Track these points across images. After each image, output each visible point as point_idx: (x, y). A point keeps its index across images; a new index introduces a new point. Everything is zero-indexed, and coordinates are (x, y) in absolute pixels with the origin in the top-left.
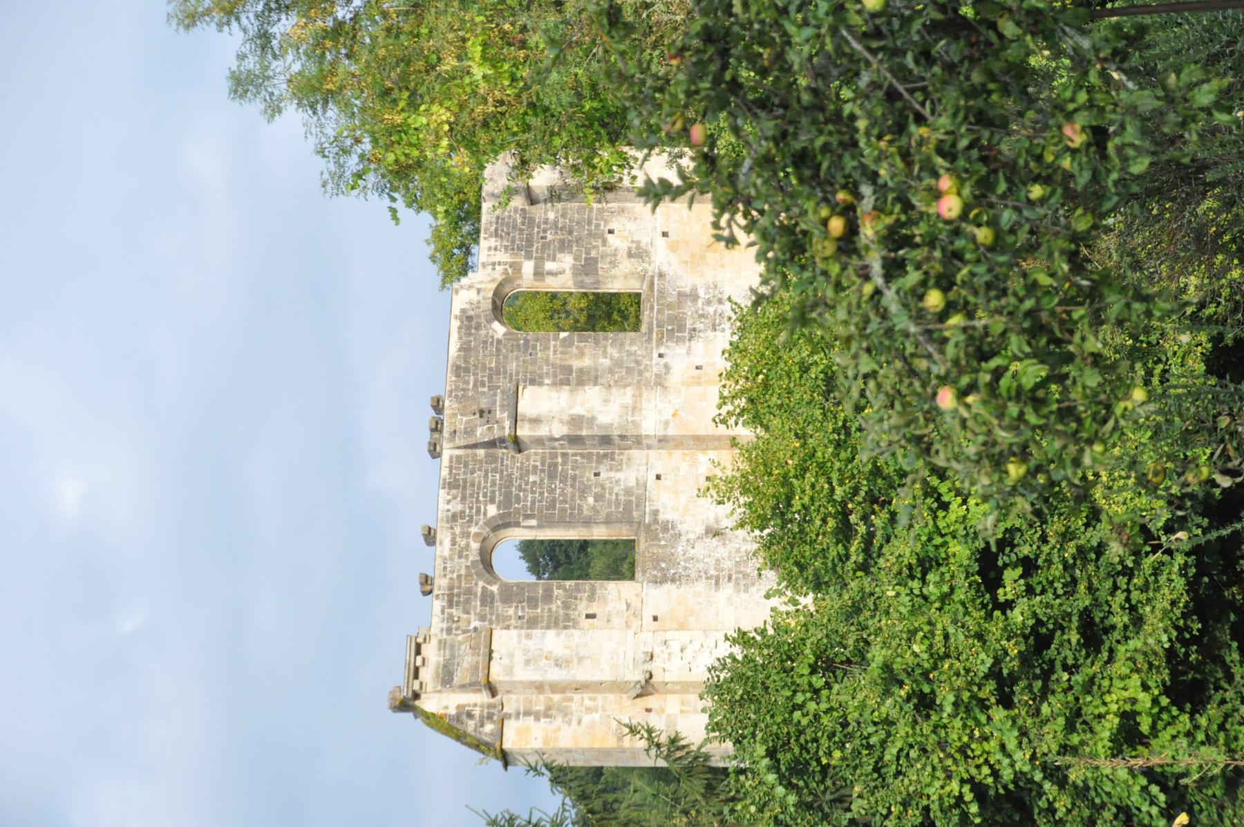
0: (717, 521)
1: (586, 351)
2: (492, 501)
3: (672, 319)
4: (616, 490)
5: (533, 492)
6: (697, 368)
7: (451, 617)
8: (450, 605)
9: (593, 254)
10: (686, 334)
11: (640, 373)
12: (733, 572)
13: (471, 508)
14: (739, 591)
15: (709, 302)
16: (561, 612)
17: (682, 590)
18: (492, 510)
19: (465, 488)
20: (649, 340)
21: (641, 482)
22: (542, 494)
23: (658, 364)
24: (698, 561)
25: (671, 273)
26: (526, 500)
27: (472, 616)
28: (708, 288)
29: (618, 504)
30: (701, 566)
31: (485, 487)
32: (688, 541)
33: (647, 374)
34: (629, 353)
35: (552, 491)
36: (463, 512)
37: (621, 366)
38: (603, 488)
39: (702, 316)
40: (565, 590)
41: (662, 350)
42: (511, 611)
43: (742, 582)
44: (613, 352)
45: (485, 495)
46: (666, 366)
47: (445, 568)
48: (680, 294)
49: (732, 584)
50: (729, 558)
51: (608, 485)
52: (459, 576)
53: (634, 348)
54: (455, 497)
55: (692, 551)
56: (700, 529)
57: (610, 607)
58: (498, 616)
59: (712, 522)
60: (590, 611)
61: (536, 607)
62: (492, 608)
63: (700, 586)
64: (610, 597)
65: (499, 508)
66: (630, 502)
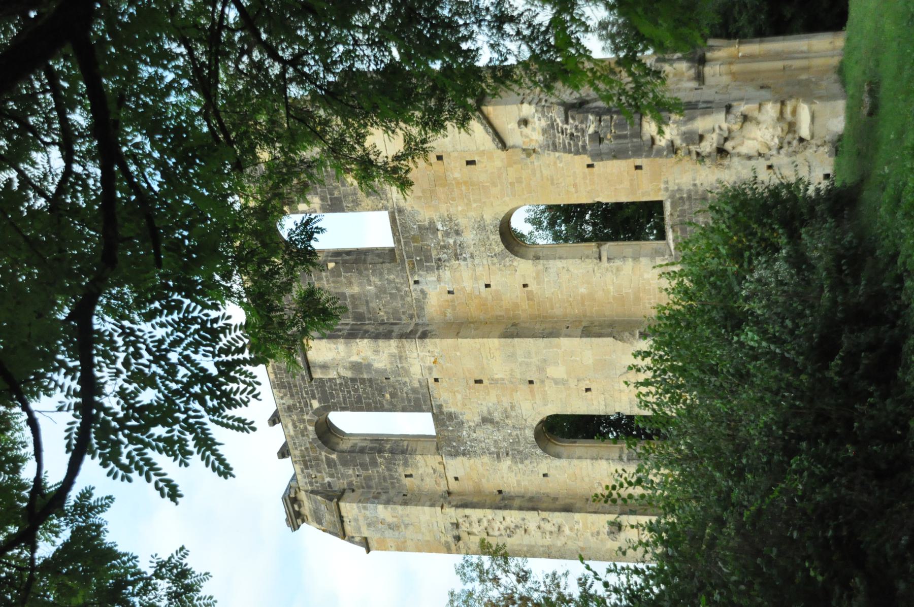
0: (490, 413)
1: (353, 280)
2: (314, 397)
3: (420, 250)
4: (405, 389)
5: (342, 391)
6: (449, 292)
7: (309, 476)
8: (307, 468)
9: (336, 194)
10: (433, 264)
11: (402, 298)
12: (509, 450)
13: (300, 402)
14: (516, 462)
15: (447, 234)
16: (387, 473)
17: (472, 461)
18: (316, 404)
19: (290, 388)
20: (403, 269)
21: (424, 384)
22: (349, 392)
23: (415, 290)
24: (481, 442)
25: (409, 209)
26: (338, 397)
27: (324, 474)
28: (443, 221)
29: (409, 400)
30: (483, 445)
31: (305, 387)
32: (470, 427)
33: (409, 299)
34: (389, 282)
35: (356, 390)
36: (294, 405)
37: (385, 292)
38: (395, 389)
39: (444, 247)
40: (385, 458)
41: (416, 279)
42: (351, 472)
43: (518, 457)
44: (375, 280)
45: (307, 393)
46: (422, 291)
47: (295, 444)
48: (420, 227)
50: (504, 440)
51: (398, 386)
52: (306, 449)
53: (392, 277)
54: (285, 395)
55: (475, 435)
56: (477, 419)
57: (421, 471)
58: (342, 474)
59: (485, 413)
60: (408, 473)
61: (367, 470)
62: (336, 469)
63: (486, 459)
64: (419, 465)
65: (320, 402)
66: (419, 399)
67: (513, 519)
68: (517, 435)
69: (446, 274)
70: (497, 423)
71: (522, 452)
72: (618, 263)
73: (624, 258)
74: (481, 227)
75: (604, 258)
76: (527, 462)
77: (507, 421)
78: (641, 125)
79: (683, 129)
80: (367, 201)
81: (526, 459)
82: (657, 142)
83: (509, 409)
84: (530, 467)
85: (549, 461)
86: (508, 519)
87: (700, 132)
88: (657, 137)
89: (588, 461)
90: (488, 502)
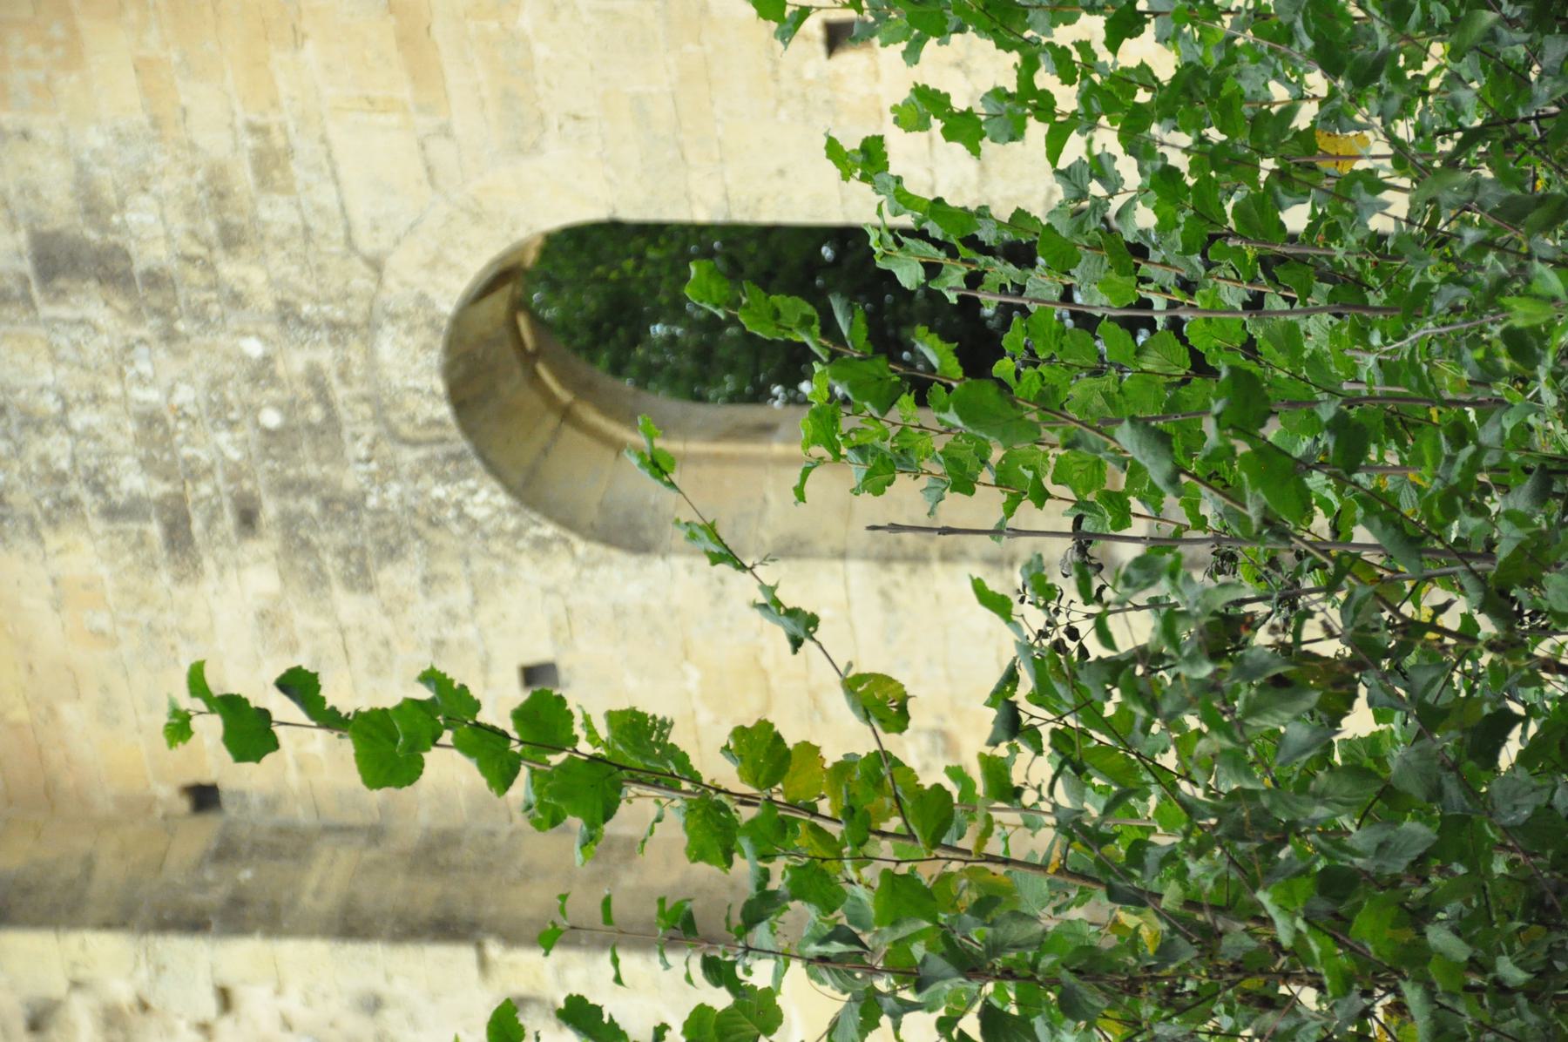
12: (258, 484)
14: (317, 581)
30: (58, 448)
49: (267, 545)
50: (219, 413)
67: (292, 1003)
68: (315, 378)
70: (155, 279)
71: (355, 503)
76: (398, 577)
77: (230, 270)
81: (392, 552)
83: (243, 177)
84: (424, 612)
85: (562, 568)
86: (256, 1001)
89: (856, 569)
90: (110, 871)
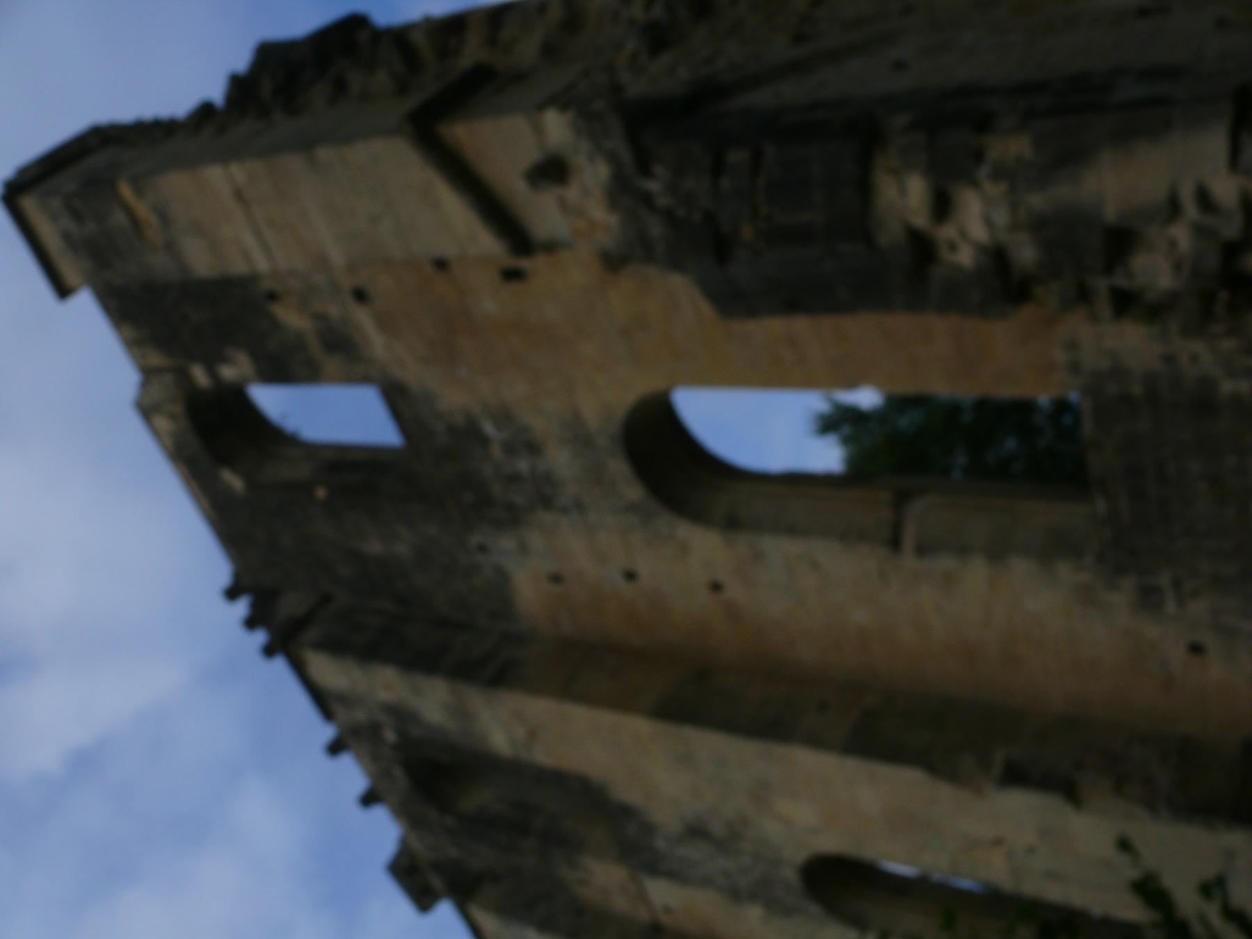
69: (536, 540)
72: (945, 562)
73: (963, 551)
74: (579, 438)
75: (908, 542)
78: (865, 187)
79: (1037, 201)
80: (331, 364)
82: (945, 254)
87: (1110, 213)
88: (946, 232)
